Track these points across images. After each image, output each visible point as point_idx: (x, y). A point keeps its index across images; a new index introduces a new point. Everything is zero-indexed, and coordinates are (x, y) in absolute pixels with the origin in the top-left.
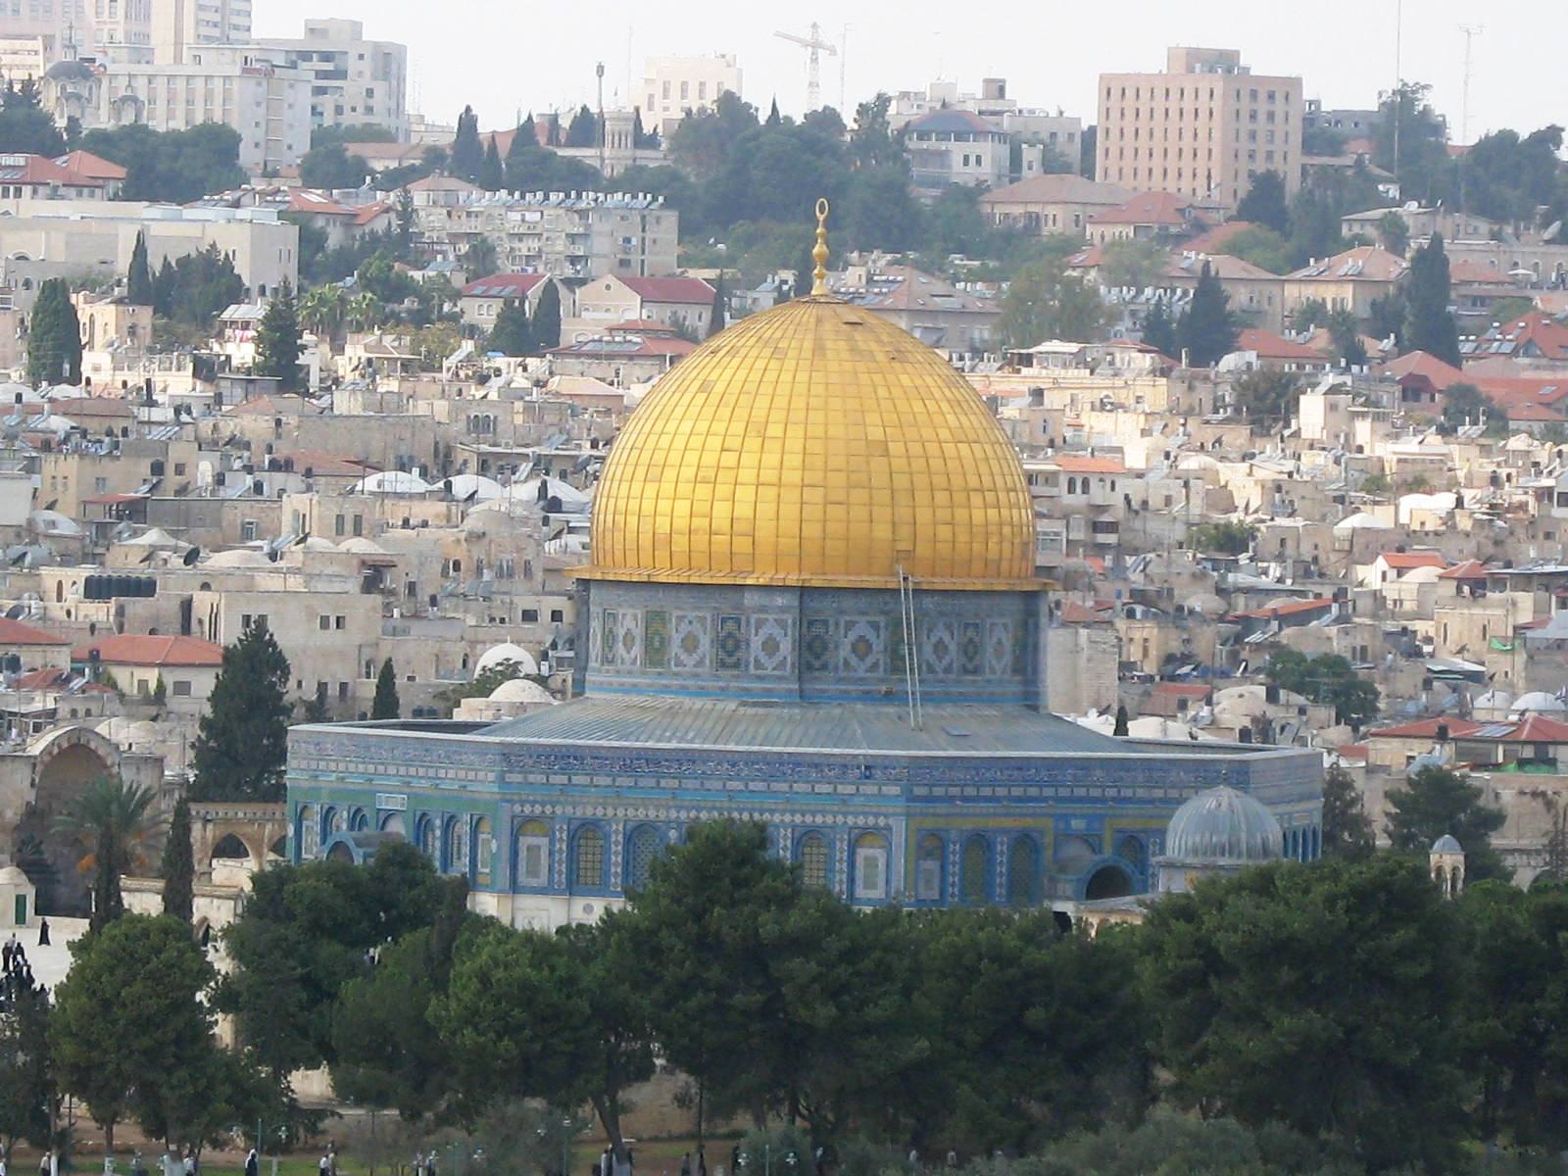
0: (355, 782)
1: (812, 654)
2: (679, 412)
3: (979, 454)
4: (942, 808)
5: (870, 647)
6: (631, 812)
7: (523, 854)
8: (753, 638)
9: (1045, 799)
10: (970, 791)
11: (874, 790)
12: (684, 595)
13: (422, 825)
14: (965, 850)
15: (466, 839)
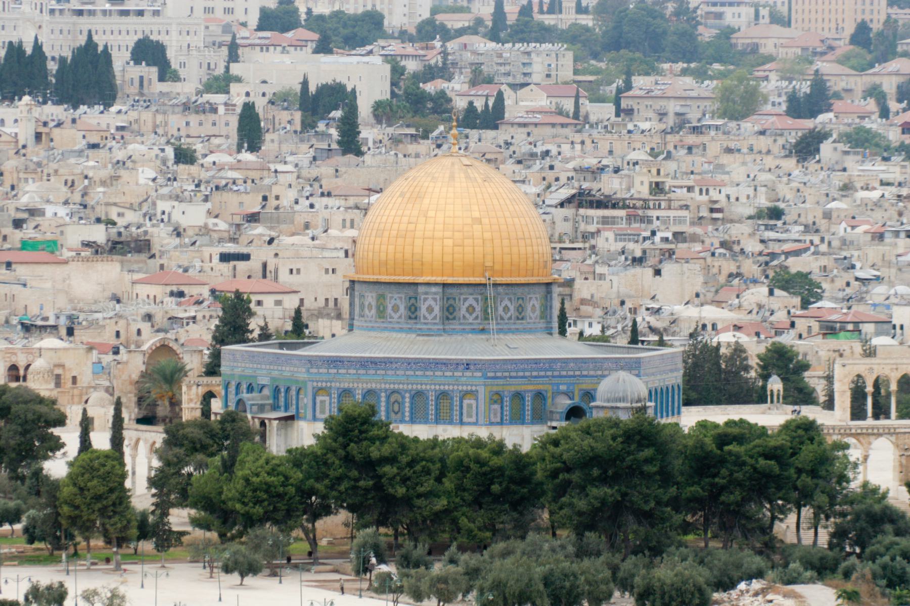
0: (248, 372)
1: (449, 313)
2: (391, 206)
3: (523, 222)
4: (501, 382)
5: (474, 309)
6: (365, 385)
7: (318, 405)
8: (422, 306)
9: (547, 377)
10: (513, 374)
11: (470, 374)
12: (393, 287)
13: (277, 390)
14: (512, 400)
15: (294, 398)
